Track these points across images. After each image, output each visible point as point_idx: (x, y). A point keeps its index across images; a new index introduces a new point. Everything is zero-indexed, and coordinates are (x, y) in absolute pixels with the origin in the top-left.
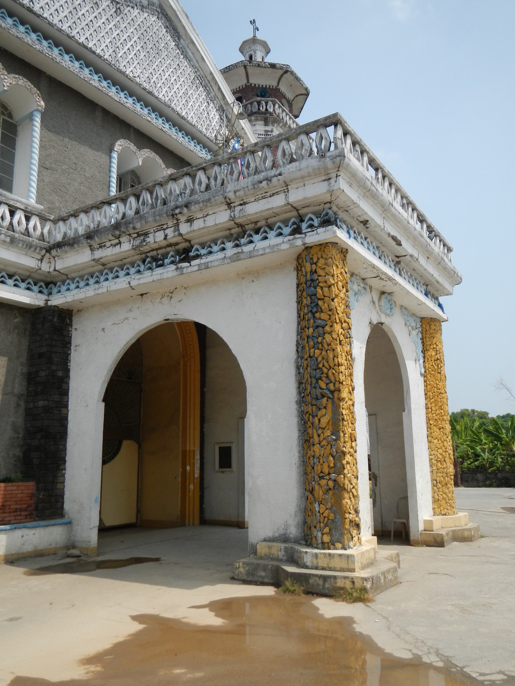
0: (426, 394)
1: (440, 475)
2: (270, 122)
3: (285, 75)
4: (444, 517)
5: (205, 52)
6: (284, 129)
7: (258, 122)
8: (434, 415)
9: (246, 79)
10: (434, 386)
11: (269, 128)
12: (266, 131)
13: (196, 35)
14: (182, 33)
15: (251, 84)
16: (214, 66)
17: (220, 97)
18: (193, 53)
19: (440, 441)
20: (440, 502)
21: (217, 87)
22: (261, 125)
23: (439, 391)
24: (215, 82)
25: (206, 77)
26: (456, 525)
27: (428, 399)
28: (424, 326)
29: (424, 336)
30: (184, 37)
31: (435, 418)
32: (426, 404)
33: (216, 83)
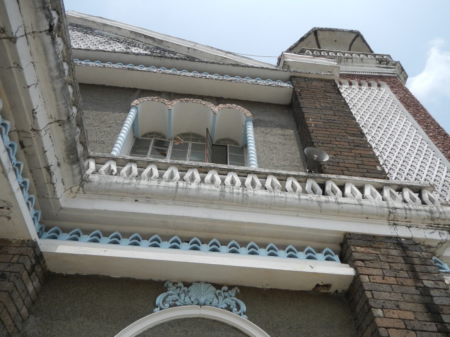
3: (320, 37)
17: (151, 42)
24: (138, 35)
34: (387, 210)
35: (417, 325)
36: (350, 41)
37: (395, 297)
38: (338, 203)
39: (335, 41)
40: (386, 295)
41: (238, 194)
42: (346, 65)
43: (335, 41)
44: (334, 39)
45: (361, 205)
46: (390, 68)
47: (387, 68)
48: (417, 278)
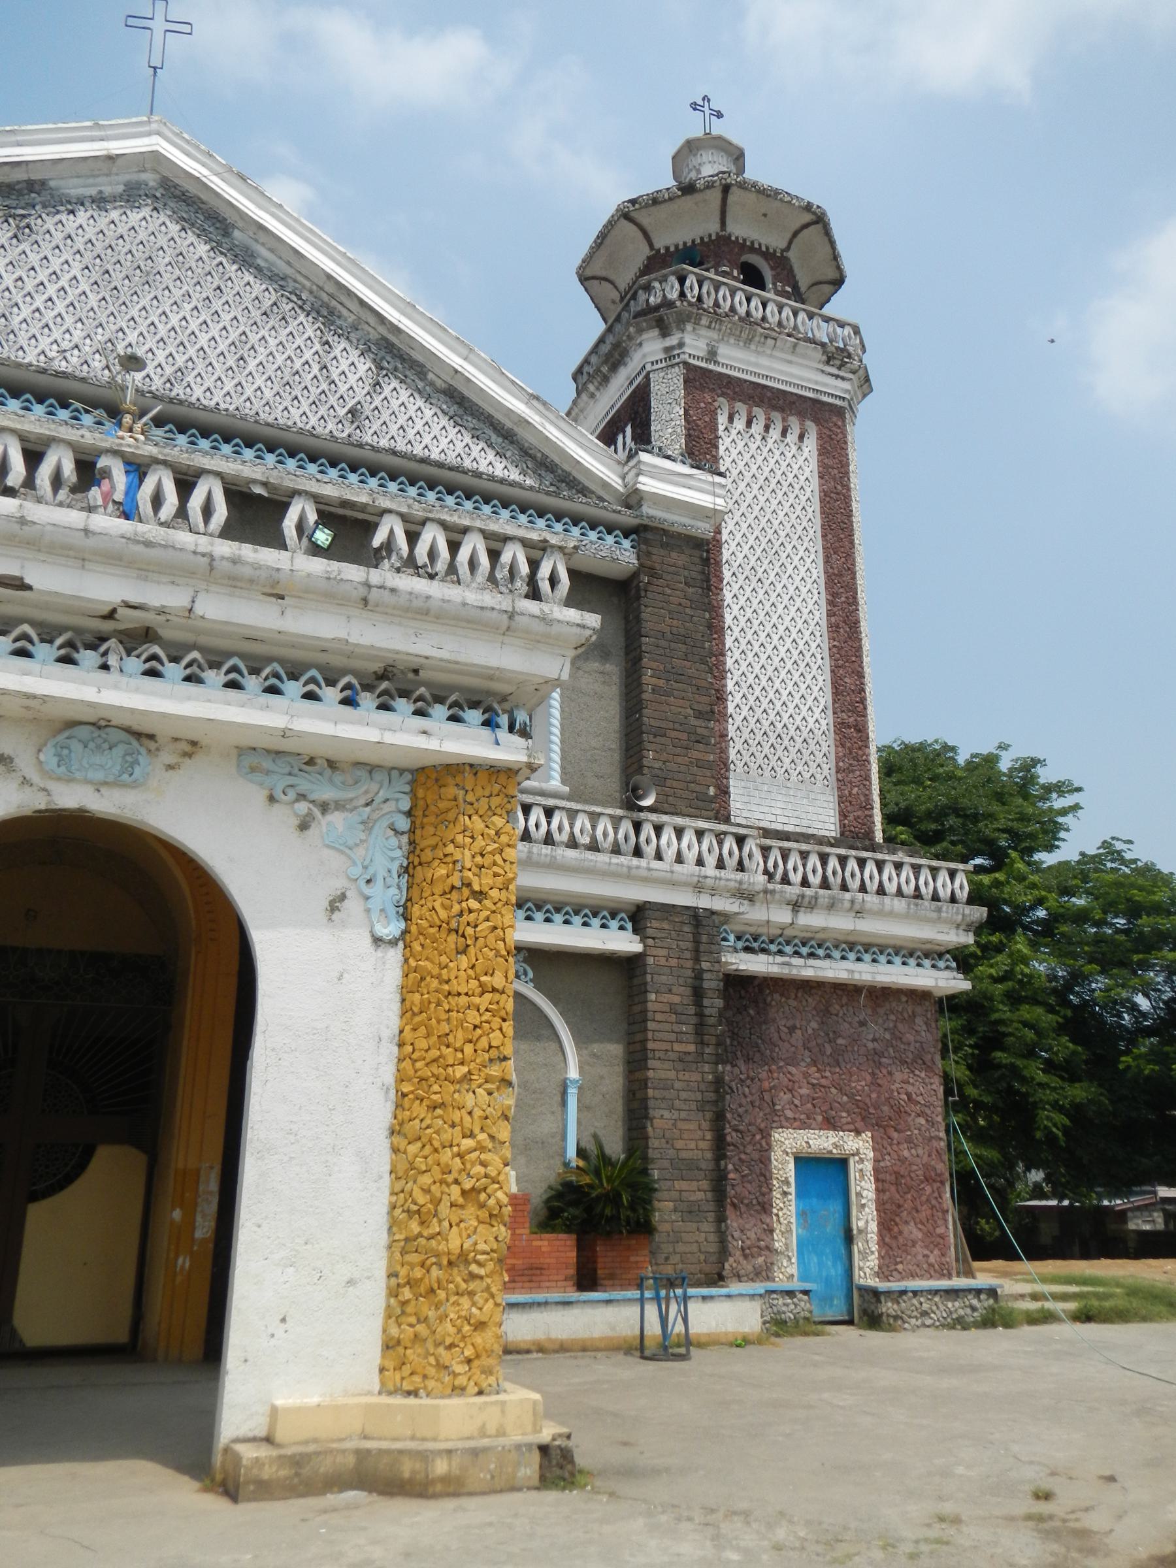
0: (403, 1000)
1: (414, 1258)
2: (674, 325)
3: (731, 199)
4: (411, 1401)
5: (308, 235)
6: (720, 330)
7: (645, 336)
8: (419, 1065)
9: (645, 242)
10: (429, 973)
11: (672, 341)
12: (667, 350)
13: (274, 210)
14: (231, 217)
15: (659, 250)
16: (339, 258)
18: (272, 250)
19: (428, 1147)
20: (400, 1350)
21: (356, 302)
22: (653, 338)
23: (446, 987)
25: (321, 288)
26: (418, 1435)
27: (408, 1015)
28: (420, 793)
29: (418, 822)
30: (240, 224)
31: (419, 1073)
32: (401, 1032)
33: (350, 293)
34: (696, 879)
35: (680, 1009)
36: (797, 225)
37: (671, 980)
38: (649, 869)
39: (765, 215)
40: (664, 979)
41: (546, 855)
42: (758, 353)
43: (765, 215)
44: (763, 211)
45: (672, 872)
46: (843, 378)
47: (837, 377)
48: (697, 960)
